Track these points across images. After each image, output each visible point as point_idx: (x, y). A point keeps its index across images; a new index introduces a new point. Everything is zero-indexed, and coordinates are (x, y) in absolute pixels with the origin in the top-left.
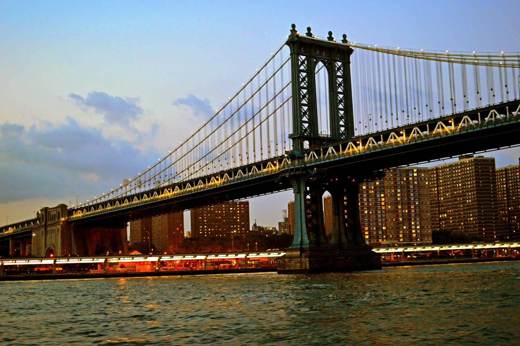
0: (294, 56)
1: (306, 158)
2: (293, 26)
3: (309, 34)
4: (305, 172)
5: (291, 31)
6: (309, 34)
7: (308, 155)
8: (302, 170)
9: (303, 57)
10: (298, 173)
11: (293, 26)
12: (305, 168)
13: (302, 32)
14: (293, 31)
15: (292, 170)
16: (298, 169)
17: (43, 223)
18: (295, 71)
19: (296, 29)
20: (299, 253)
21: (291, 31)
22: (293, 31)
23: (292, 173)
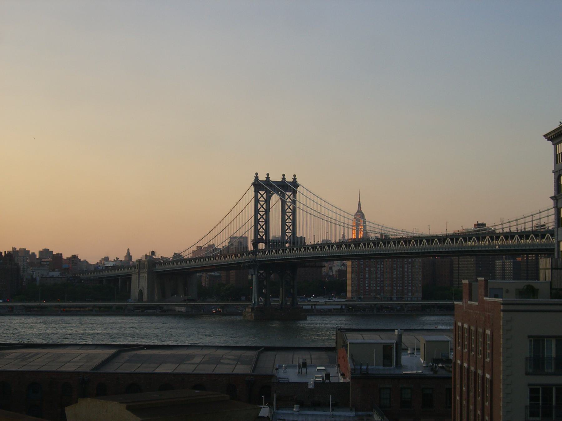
0: (257, 192)
1: (258, 255)
2: (257, 174)
3: (268, 178)
4: (255, 264)
6: (268, 178)
7: (259, 253)
9: (262, 193)
10: (252, 264)
11: (257, 174)
12: (255, 261)
13: (262, 178)
14: (257, 177)
16: (252, 262)
17: (137, 271)
18: (257, 201)
19: (258, 176)
20: (250, 310)
22: (257, 177)
23: (249, 264)
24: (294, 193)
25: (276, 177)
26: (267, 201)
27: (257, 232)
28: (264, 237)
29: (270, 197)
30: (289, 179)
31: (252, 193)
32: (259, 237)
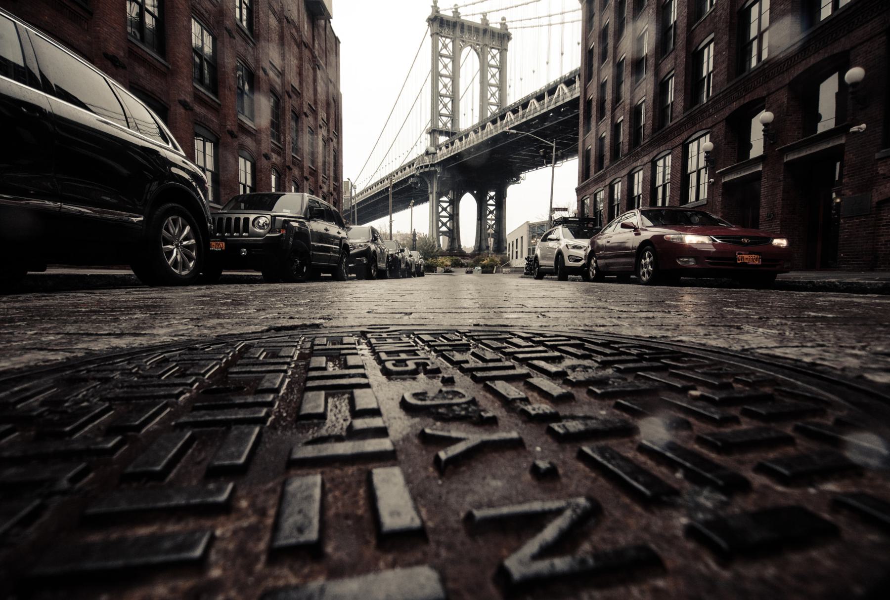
5: (432, 6)
6: (456, 12)
8: (431, 167)
10: (427, 170)
14: (435, 8)
15: (422, 167)
18: (436, 55)
19: (438, 5)
21: (432, 6)
22: (435, 8)
23: (422, 171)
24: (503, 51)
25: (471, 15)
26: (455, 58)
27: (436, 114)
28: (449, 125)
29: (461, 49)
30: (494, 23)
31: (429, 40)
32: (441, 125)
